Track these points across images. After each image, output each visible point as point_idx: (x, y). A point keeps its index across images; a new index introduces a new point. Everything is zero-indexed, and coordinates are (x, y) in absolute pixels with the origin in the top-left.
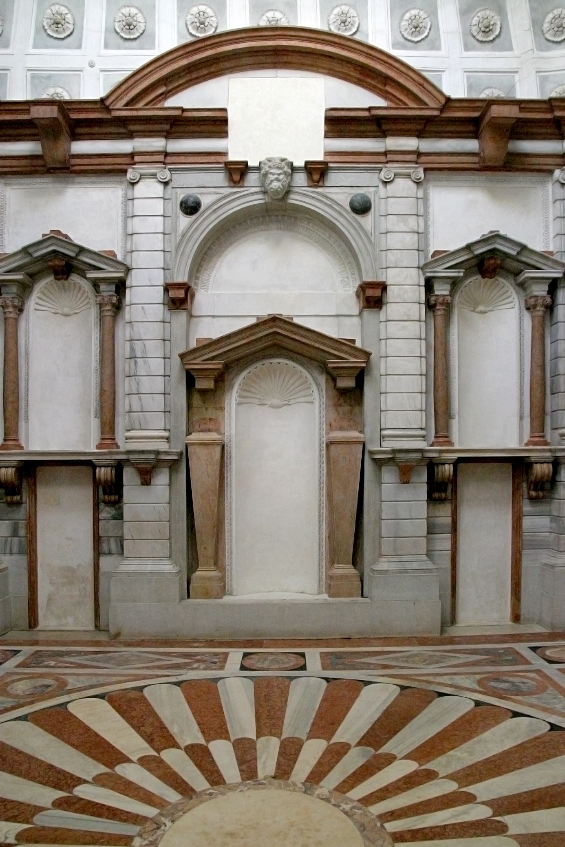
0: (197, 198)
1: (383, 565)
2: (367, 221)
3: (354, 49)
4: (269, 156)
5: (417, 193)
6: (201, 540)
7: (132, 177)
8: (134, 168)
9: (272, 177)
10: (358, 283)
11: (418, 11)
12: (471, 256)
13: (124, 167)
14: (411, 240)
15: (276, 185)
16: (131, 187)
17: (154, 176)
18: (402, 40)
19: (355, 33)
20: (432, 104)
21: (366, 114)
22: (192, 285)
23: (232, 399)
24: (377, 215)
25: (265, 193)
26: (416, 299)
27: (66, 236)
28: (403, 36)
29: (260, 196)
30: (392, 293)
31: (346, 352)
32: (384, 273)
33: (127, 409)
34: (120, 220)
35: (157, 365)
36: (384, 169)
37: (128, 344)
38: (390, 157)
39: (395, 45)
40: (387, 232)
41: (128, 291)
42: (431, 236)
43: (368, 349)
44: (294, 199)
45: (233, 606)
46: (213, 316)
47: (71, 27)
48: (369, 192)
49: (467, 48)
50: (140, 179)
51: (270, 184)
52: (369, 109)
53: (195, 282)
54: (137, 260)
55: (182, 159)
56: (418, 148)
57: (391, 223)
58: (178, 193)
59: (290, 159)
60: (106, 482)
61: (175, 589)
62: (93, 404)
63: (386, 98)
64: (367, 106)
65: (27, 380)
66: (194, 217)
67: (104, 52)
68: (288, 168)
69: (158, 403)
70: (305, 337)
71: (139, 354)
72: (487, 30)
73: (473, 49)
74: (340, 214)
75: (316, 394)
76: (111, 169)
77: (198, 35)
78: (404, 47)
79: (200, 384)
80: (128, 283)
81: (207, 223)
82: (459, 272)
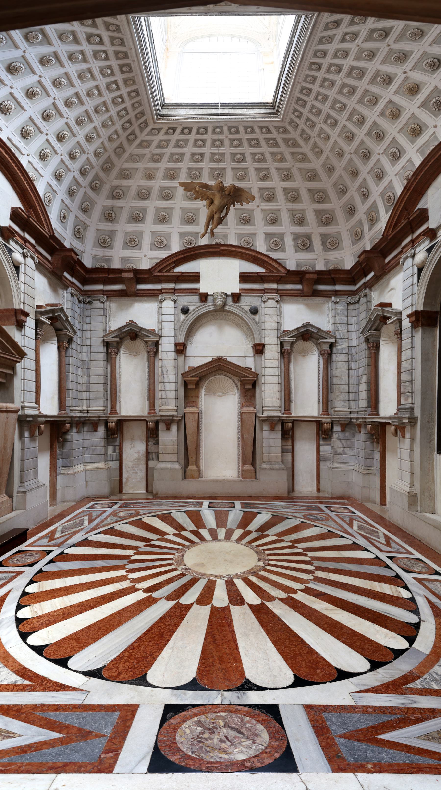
1: (264, 466)
2: (257, 317)
4: (217, 291)
6: (190, 455)
10: (253, 343)
14: (274, 325)
15: (219, 303)
17: (170, 298)
23: (203, 392)
25: (215, 305)
26: (276, 351)
27: (135, 323)
29: (213, 307)
30: (267, 348)
31: (248, 373)
33: (160, 397)
34: (156, 315)
35: (172, 378)
37: (160, 369)
38: (266, 291)
41: (160, 346)
42: (282, 323)
43: (257, 372)
44: (227, 308)
45: (204, 481)
48: (258, 305)
52: (258, 273)
54: (164, 333)
57: (266, 318)
60: (152, 428)
61: (180, 475)
62: (146, 395)
65: (120, 385)
66: (186, 315)
69: (172, 394)
70: (232, 367)
71: (165, 373)
72: (304, 245)
75: (236, 391)
79: (190, 387)
80: (160, 342)
81: (192, 317)
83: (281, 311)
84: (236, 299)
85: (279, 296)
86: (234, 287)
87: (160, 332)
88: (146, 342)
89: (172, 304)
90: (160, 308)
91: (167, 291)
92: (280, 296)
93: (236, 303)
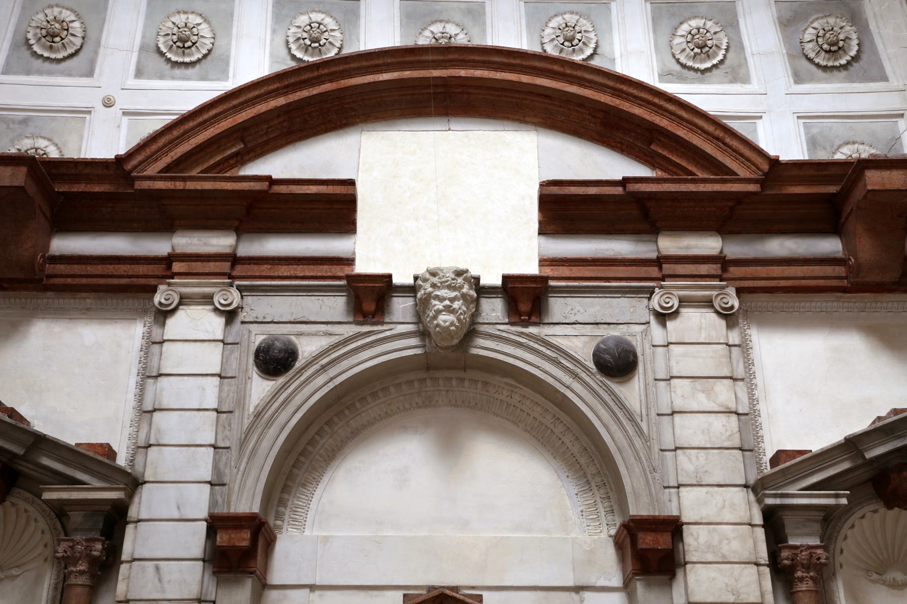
0: (291, 343)
3: (590, 81)
4: (432, 266)
5: (727, 336)
7: (163, 301)
8: (169, 284)
9: (439, 306)
10: (618, 521)
11: (703, 21)
12: (860, 462)
13: (152, 282)
14: (725, 429)
15: (445, 319)
16: (161, 319)
17: (207, 299)
18: (678, 68)
19: (591, 57)
20: (743, 173)
21: (619, 190)
22: (271, 521)
24: (650, 379)
28: (678, 61)
29: (414, 341)
30: (695, 541)
32: (674, 499)
36: (657, 290)
38: (668, 268)
39: (665, 75)
40: (673, 413)
41: (130, 529)
42: (763, 419)
44: (483, 348)
46: (312, 588)
47: (78, 42)
48: (633, 335)
49: (798, 78)
50: (180, 303)
51: (435, 317)
52: (626, 181)
53: (277, 512)
54: (158, 464)
55: (265, 269)
56: (721, 252)
57: (682, 394)
58: (254, 333)
59: (474, 272)
63: (652, 165)
64: (619, 177)
66: (281, 380)
67: (132, 82)
68: (471, 288)
73: (812, 79)
74: (576, 376)
76: (126, 289)
77: (306, 58)
78: (681, 79)
80: (132, 513)
81: (307, 390)
82: (837, 496)
83: (748, 363)
84: (524, 307)
85: (732, 291)
86: (516, 247)
87: (139, 459)
88: (60, 510)
89: (214, 325)
90: (153, 343)
91: (198, 267)
92: (739, 291)
93: (526, 324)
